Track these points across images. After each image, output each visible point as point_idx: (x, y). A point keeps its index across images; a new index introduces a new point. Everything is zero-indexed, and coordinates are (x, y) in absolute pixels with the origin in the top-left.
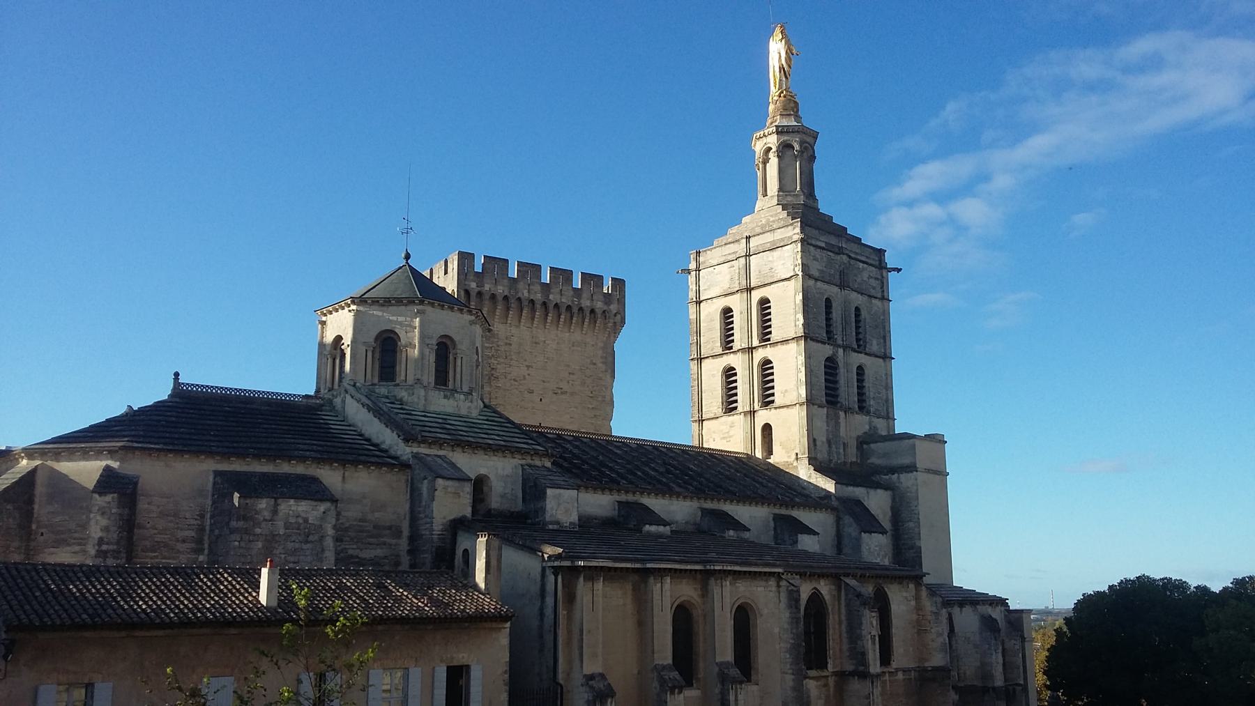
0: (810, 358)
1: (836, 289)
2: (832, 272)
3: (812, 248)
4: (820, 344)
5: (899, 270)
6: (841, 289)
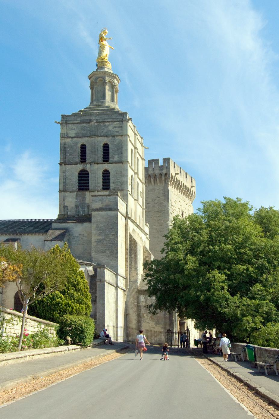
0: (64, 172)
1: (87, 139)
2: (85, 132)
3: (70, 126)
5: (130, 119)
6: (90, 138)
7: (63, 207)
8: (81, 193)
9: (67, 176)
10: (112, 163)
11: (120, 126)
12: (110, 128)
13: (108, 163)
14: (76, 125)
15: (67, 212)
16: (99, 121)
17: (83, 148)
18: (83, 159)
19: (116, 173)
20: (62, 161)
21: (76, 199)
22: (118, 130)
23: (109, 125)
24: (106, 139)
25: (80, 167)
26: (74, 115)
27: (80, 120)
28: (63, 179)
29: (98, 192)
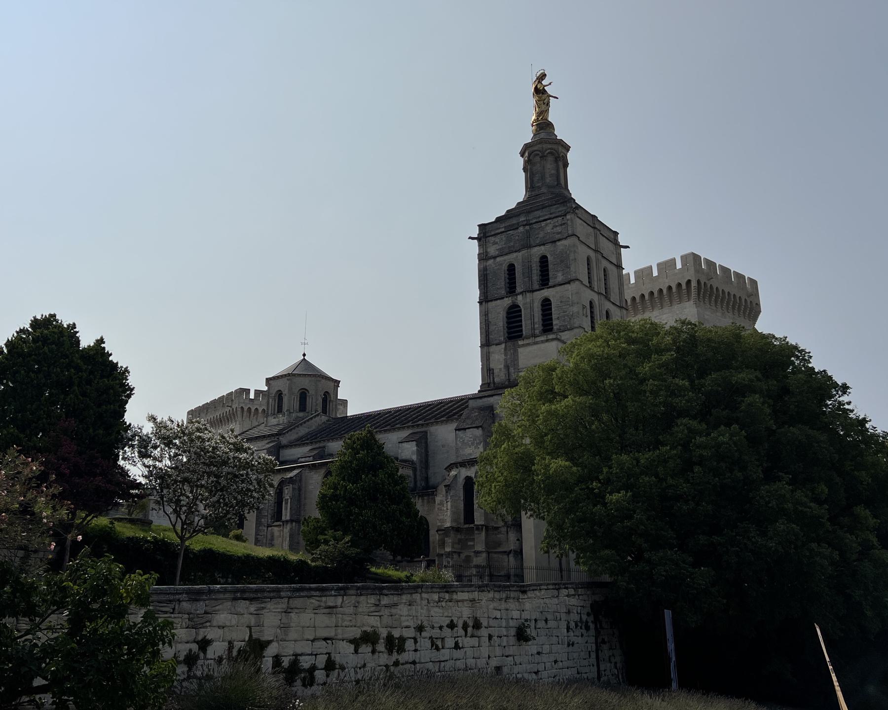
1: (515, 255)
2: (512, 244)
3: (492, 239)
4: (498, 301)
7: (487, 370)
8: (510, 344)
9: (490, 320)
10: (554, 286)
11: (563, 222)
12: (549, 229)
13: (548, 288)
14: (499, 235)
15: (494, 378)
16: (530, 222)
17: (511, 268)
18: (511, 289)
19: (561, 302)
20: (482, 298)
21: (506, 355)
22: (560, 231)
23: (546, 225)
24: (543, 249)
25: (508, 302)
26: (499, 220)
27: (505, 227)
28: (484, 326)
29: (537, 337)
